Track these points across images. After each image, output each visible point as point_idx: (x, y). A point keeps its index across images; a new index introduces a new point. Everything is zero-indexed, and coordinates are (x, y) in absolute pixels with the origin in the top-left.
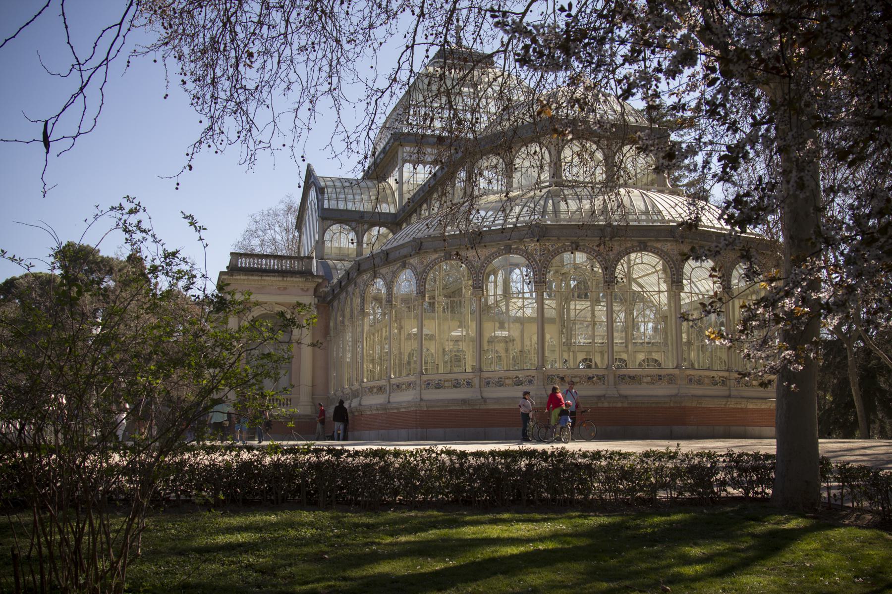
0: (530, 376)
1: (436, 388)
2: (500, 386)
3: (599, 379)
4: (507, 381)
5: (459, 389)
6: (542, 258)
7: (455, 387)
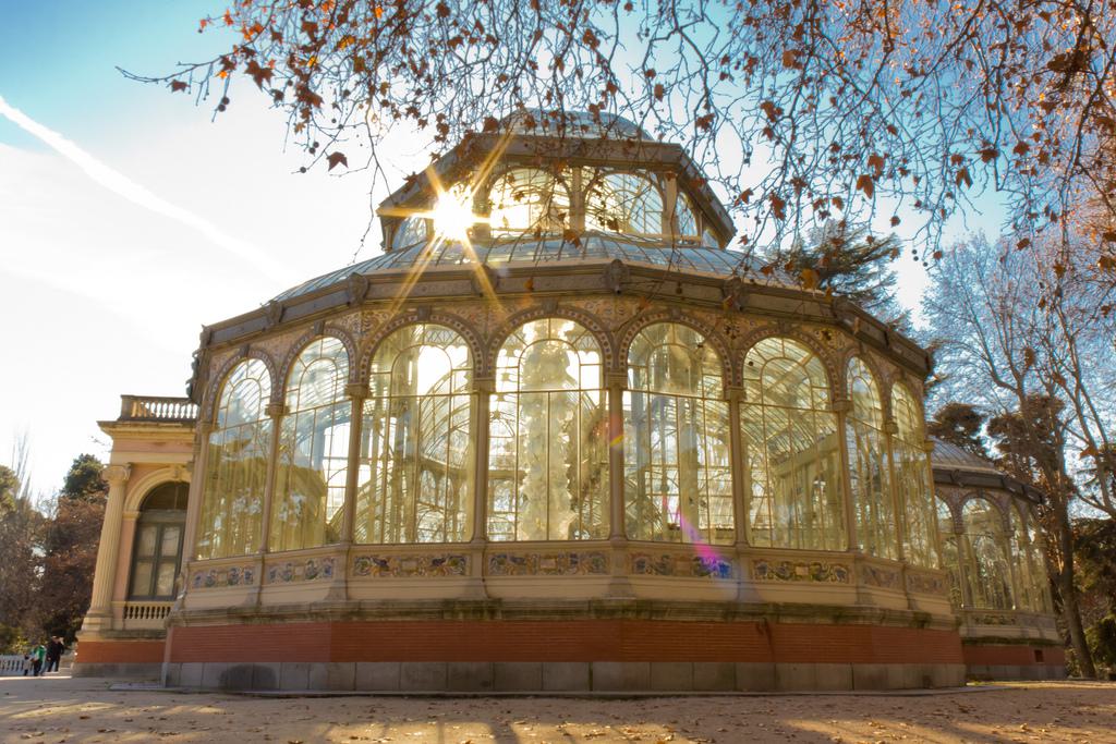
0: (328, 559)
1: (208, 585)
2: (288, 580)
3: (455, 564)
4: (297, 569)
5: (234, 587)
6: (364, 338)
7: (231, 583)
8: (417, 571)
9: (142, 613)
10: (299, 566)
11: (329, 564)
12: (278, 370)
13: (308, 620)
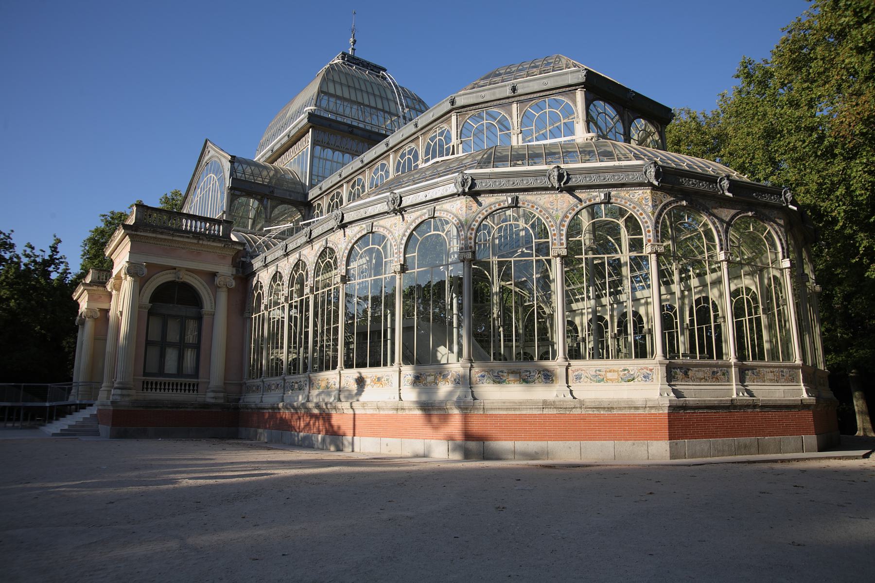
0: (647, 369)
2: (599, 381)
3: (724, 374)
8: (704, 378)
9: (156, 386)
10: (610, 371)
11: (648, 372)
12: (558, 222)
13: (641, 412)
